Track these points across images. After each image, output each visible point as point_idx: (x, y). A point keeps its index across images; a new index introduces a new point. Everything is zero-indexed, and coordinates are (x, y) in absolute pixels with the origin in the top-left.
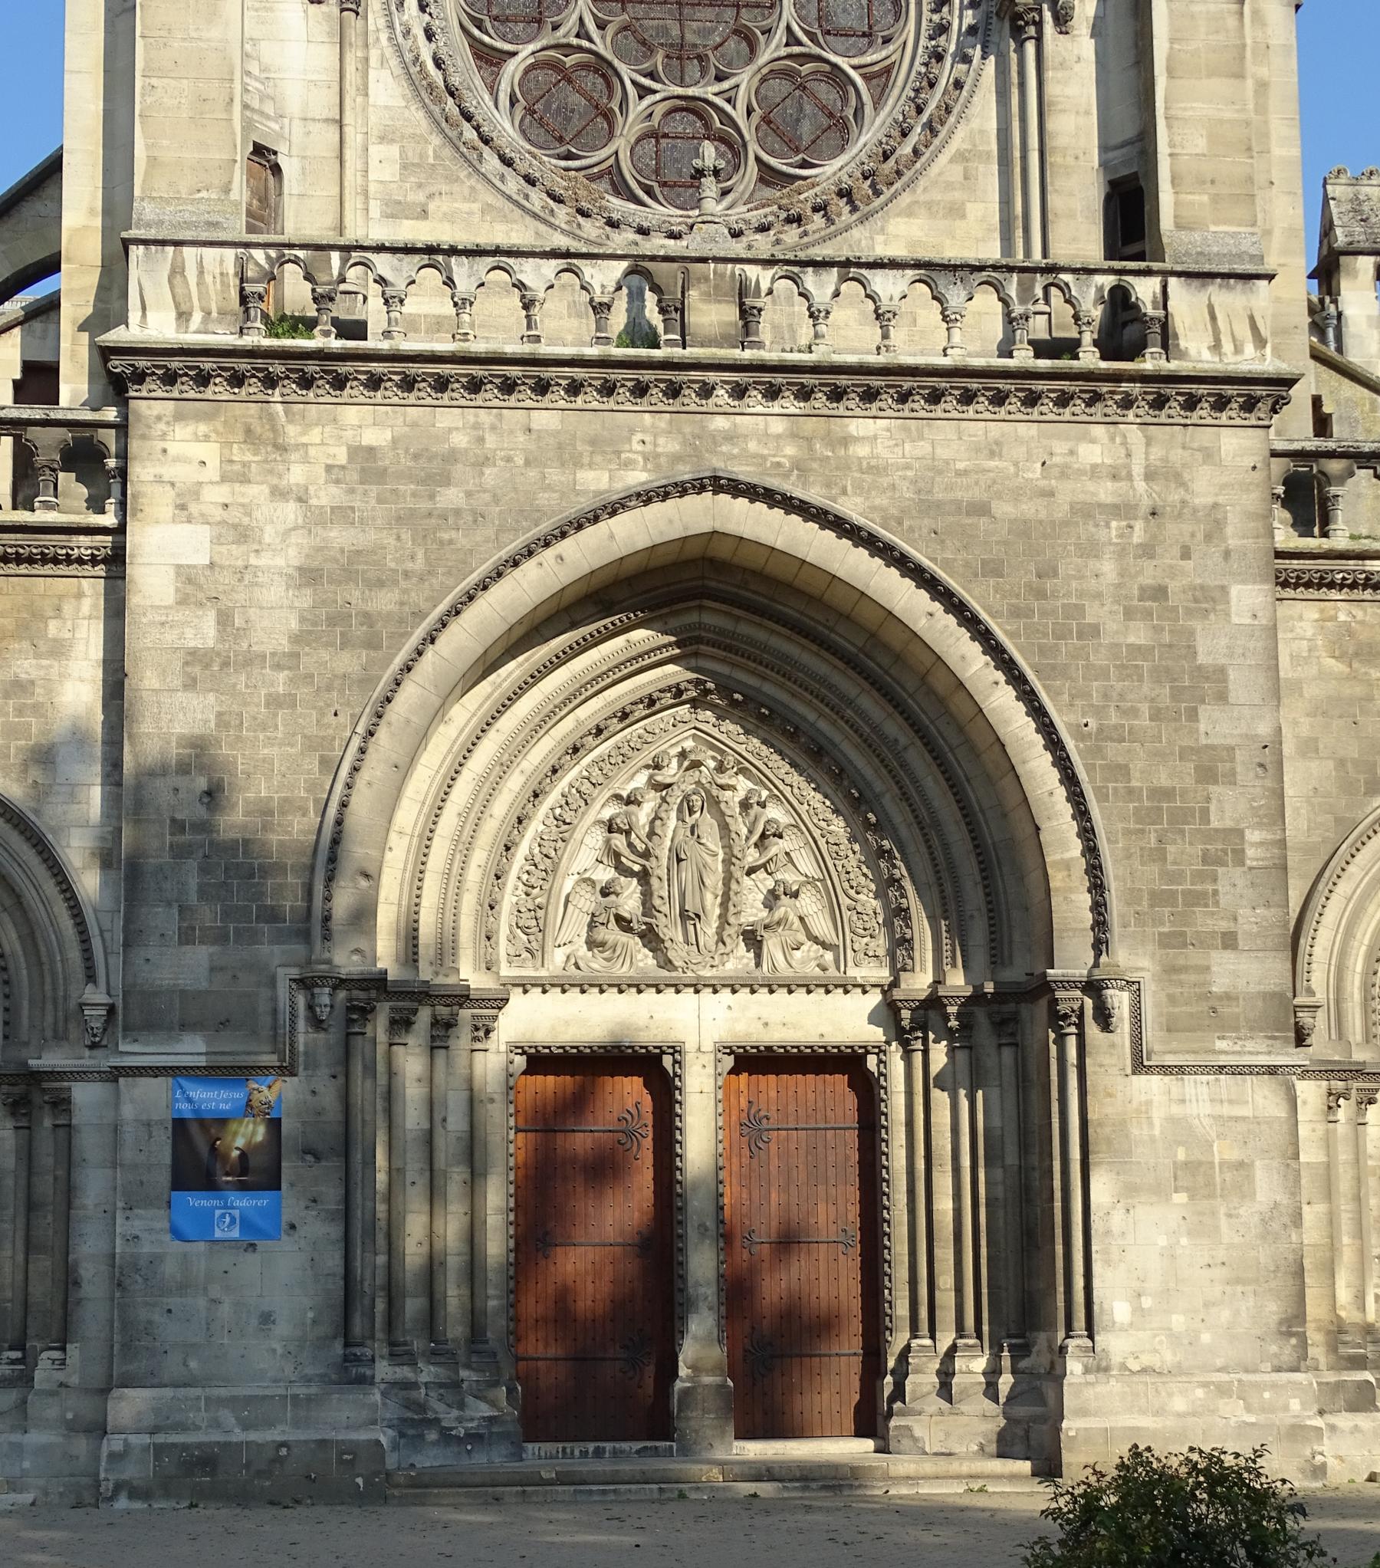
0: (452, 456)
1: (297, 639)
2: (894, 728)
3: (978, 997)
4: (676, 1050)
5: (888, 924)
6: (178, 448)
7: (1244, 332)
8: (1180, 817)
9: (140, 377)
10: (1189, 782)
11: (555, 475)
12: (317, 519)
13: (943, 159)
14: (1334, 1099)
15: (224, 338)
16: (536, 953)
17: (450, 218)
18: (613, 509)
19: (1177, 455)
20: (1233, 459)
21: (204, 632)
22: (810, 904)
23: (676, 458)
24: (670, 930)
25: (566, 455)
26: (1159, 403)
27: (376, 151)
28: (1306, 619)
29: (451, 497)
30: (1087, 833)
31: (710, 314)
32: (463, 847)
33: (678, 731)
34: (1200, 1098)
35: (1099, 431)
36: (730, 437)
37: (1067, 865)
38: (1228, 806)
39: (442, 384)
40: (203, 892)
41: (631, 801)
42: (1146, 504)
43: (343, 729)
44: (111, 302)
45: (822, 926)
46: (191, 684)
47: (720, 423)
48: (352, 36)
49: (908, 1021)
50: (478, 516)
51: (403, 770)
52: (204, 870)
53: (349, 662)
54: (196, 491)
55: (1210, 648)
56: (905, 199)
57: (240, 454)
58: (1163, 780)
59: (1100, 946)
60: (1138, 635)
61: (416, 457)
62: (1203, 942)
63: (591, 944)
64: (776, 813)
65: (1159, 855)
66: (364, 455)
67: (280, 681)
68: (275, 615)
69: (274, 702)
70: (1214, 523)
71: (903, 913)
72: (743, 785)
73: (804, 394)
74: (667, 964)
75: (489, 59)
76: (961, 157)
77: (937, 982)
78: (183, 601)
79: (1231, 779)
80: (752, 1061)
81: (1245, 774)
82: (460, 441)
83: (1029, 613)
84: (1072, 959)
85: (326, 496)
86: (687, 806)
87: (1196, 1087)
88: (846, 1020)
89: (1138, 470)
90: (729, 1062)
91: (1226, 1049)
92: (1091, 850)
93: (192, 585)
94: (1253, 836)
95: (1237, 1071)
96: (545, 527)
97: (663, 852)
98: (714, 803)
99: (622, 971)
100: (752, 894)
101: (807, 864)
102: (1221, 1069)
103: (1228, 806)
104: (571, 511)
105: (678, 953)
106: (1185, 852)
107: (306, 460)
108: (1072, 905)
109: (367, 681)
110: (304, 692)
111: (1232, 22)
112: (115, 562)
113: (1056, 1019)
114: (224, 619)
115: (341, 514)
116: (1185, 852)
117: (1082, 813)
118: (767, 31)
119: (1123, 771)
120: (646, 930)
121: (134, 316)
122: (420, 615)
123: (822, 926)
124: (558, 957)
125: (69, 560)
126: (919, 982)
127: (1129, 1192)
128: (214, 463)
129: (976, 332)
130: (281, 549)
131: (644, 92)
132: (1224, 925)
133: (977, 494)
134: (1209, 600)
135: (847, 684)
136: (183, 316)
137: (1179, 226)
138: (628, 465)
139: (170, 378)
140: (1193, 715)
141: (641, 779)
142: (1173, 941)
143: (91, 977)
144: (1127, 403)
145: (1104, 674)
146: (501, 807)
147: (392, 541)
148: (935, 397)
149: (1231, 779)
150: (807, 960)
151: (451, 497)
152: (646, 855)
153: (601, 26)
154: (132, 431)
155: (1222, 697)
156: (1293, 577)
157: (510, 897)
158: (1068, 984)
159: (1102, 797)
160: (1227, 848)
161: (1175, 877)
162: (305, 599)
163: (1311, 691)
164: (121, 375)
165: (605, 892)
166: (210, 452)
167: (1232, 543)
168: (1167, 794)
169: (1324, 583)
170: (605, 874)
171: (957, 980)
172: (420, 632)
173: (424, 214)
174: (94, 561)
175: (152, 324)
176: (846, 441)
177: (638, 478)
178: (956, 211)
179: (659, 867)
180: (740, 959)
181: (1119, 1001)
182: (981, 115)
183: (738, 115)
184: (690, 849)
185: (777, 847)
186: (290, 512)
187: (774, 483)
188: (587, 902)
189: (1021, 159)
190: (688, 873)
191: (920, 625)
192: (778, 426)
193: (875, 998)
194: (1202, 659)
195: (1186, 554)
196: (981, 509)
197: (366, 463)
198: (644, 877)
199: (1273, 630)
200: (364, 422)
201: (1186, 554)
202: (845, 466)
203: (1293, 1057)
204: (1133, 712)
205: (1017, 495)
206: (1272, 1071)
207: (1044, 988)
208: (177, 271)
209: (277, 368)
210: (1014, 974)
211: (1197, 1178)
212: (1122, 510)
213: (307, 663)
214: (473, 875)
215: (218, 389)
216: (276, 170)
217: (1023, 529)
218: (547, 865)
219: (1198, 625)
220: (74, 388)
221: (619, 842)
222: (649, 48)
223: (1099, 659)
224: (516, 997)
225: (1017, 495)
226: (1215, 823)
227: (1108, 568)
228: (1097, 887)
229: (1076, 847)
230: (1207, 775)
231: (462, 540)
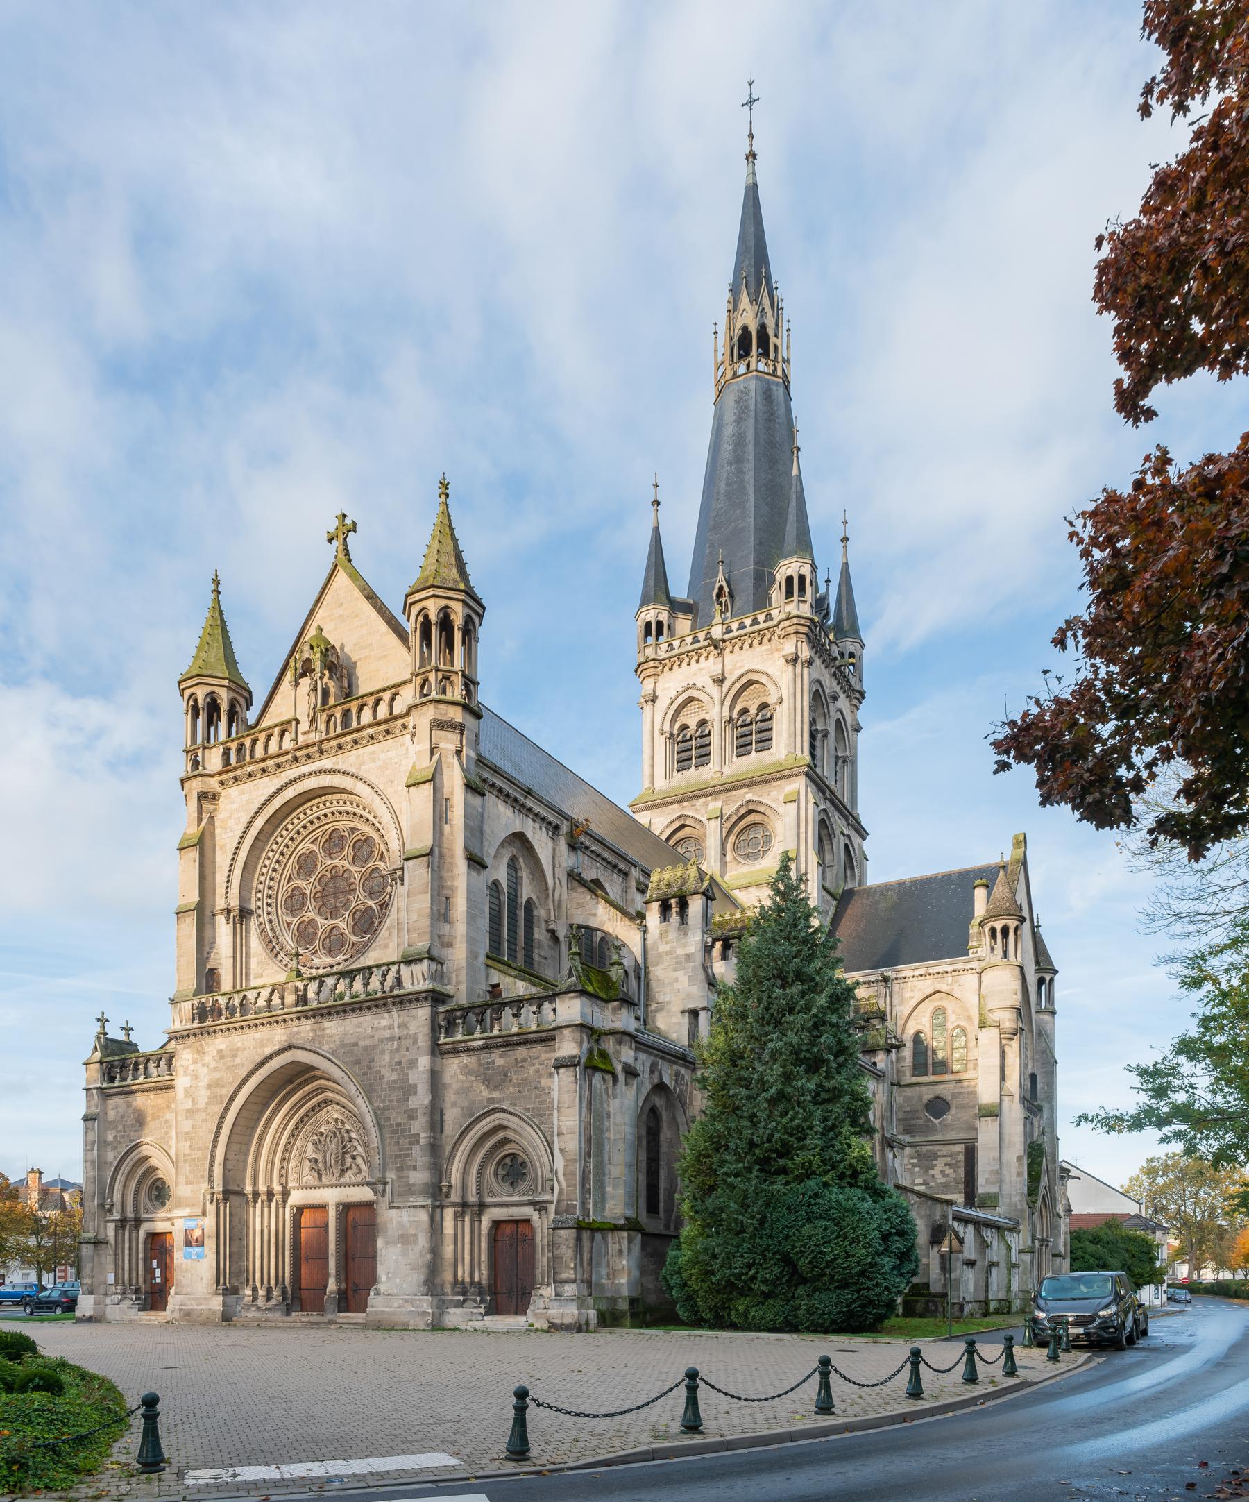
0: (237, 1050)
6: (184, 1056)
7: (420, 977)
8: (403, 1131)
11: (259, 1051)
19: (406, 1019)
21: (189, 1105)
29: (238, 1060)
34: (405, 1215)
35: (386, 1015)
36: (297, 1033)
47: (295, 1029)
54: (187, 1068)
55: (413, 1078)
57: (197, 1056)
58: (399, 1121)
60: (394, 1077)
62: (408, 1169)
65: (397, 1143)
66: (220, 1051)
68: (203, 1096)
69: (203, 1121)
73: (314, 1016)
76: (388, 928)
79: (417, 1118)
81: (420, 1116)
82: (239, 1045)
87: (405, 1212)
91: (413, 1201)
94: (422, 1135)
95: (414, 1207)
106: (404, 1142)
115: (216, 1069)
116: (404, 1142)
119: (389, 1119)
127: (387, 1243)
134: (413, 1063)
142: (400, 1169)
149: (417, 1118)
155: (415, 1093)
161: (401, 1150)
163: (456, 1086)
166: (190, 1056)
168: (399, 1125)
178: (386, 946)
186: (205, 1070)
192: (308, 1028)
196: (356, 1044)
200: (219, 1043)
202: (323, 1036)
204: (391, 1101)
205: (365, 1038)
206: (423, 1207)
211: (404, 1239)
212: (391, 1039)
217: (366, 1048)
225: (365, 1038)
227: (387, 1057)
230: (411, 1118)
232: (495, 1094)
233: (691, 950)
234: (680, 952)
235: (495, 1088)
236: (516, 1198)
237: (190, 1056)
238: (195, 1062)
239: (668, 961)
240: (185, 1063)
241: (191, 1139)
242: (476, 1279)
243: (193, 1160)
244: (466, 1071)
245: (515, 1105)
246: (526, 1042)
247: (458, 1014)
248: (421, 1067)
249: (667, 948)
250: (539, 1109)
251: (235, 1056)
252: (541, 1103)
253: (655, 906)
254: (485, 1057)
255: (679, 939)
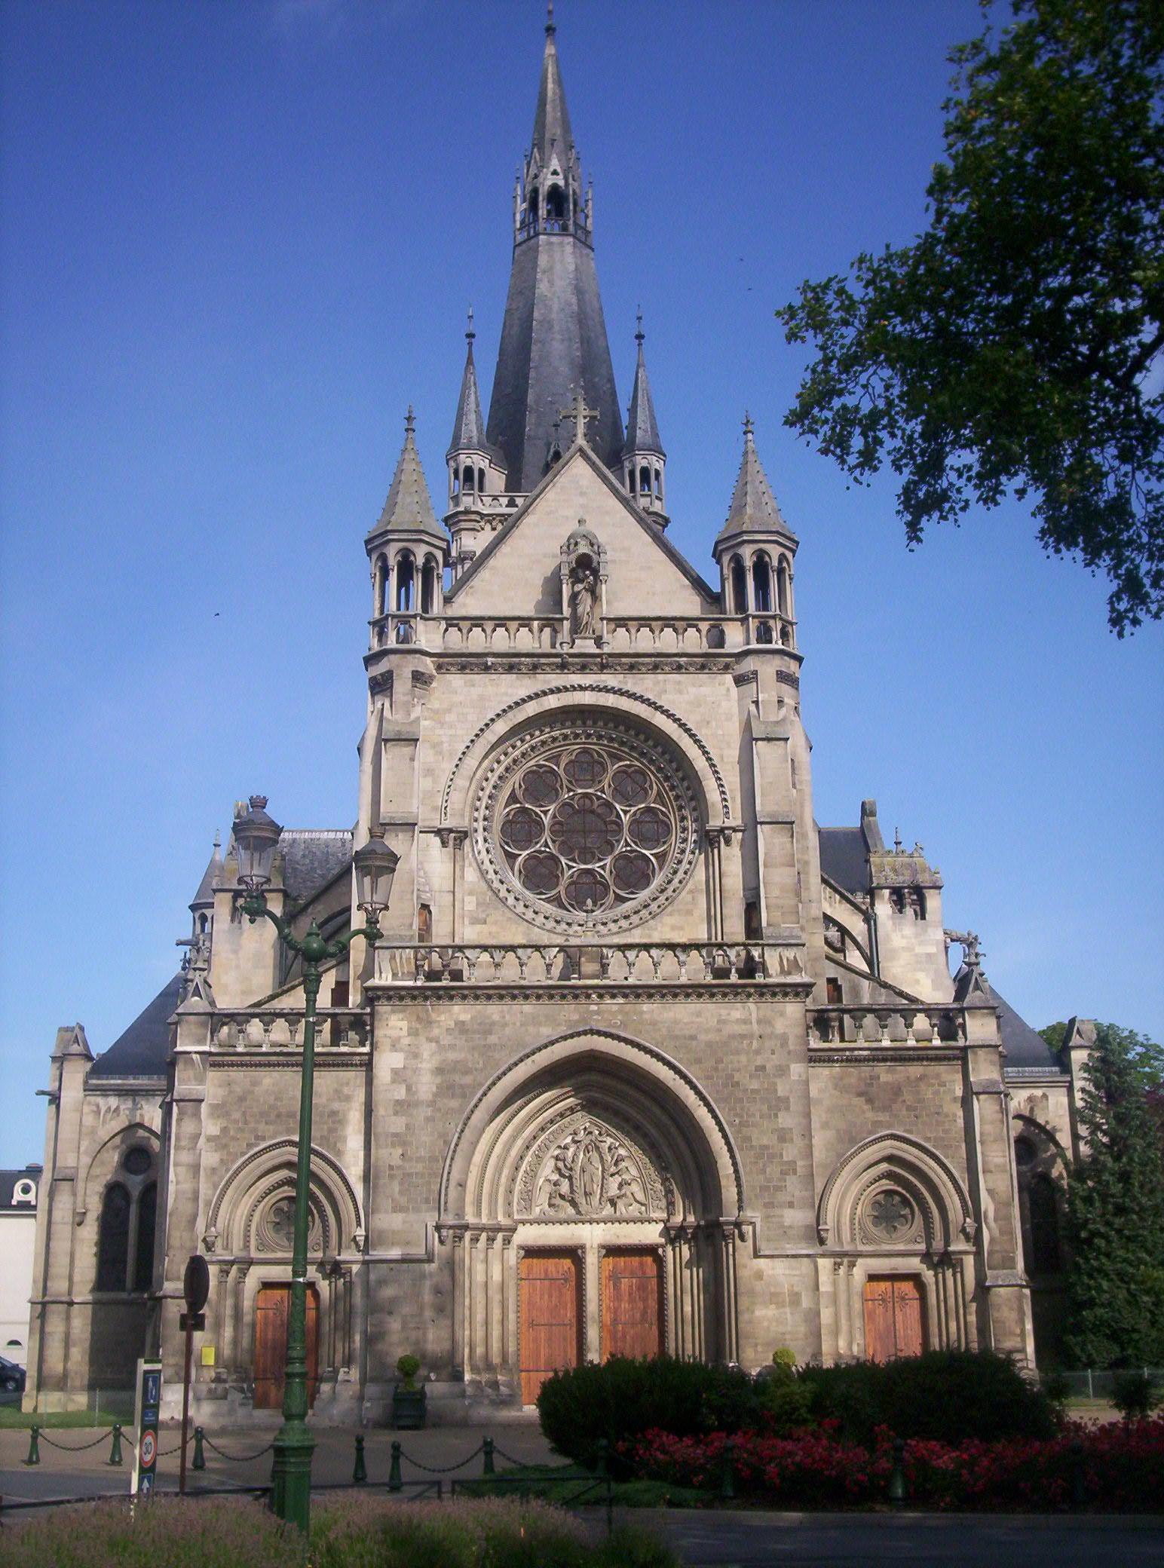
0: (493, 1023)
1: (435, 1095)
2: (665, 1119)
3: (698, 1226)
4: (583, 1247)
5: (666, 1196)
6: (393, 1024)
8: (771, 1157)
9: (379, 998)
10: (775, 1142)
11: (531, 1029)
12: (442, 1048)
13: (684, 893)
14: (837, 1266)
15: (410, 983)
16: (528, 1208)
17: (495, 923)
18: (552, 1043)
20: (791, 1013)
21: (401, 1093)
22: (635, 1188)
23: (577, 1021)
24: (581, 1200)
25: (535, 1021)
26: (762, 995)
27: (467, 899)
28: (823, 1075)
29: (493, 1039)
30: (735, 1164)
31: (589, 967)
32: (499, 1170)
33: (582, 1121)
36: (597, 1013)
37: (728, 1176)
38: (791, 1152)
39: (489, 997)
40: (401, 1192)
41: (566, 1148)
42: (757, 1033)
43: (454, 1128)
44: (368, 972)
45: (640, 1196)
46: (396, 1113)
47: (594, 1008)
48: (458, 858)
49: (674, 1235)
50: (503, 1046)
51: (474, 1145)
52: (401, 1184)
53: (454, 1103)
56: (670, 908)
58: (765, 1142)
59: (740, 1208)
60: (755, 1085)
61: (480, 1024)
62: (781, 1206)
63: (550, 1205)
64: (622, 1152)
67: (429, 1112)
68: (426, 1086)
70: (784, 1039)
71: (671, 1192)
72: (609, 1140)
73: (625, 996)
74: (579, 1213)
75: (511, 858)
76: (691, 892)
77: (684, 1219)
78: (393, 1081)
80: (613, 1251)
82: (496, 1017)
83: (712, 1078)
84: (730, 1214)
85: (446, 1040)
86: (587, 1150)
88: (651, 1234)
89: (754, 1021)
90: (604, 1252)
92: (736, 1171)
93: (397, 1075)
94: (800, 1163)
96: (528, 1050)
97: (578, 1169)
98: (597, 1148)
99: (562, 1215)
100: (613, 1184)
101: (634, 1171)
102: (787, 1256)
103: (791, 1152)
104: (535, 1046)
105: (583, 1208)
107: (439, 1027)
108: (729, 1193)
109: (461, 1110)
110: (438, 1115)
111: (789, 845)
112: (368, 1065)
113: (725, 1237)
114: (409, 1089)
115: (452, 1047)
117: (733, 1157)
118: (618, 841)
119: (749, 1139)
120: (571, 1201)
121: (377, 975)
122: (481, 1085)
123: (640, 1196)
124: (538, 1210)
125: (352, 1065)
126: (678, 1219)
128: (405, 1029)
129: (694, 969)
130: (429, 1059)
131: (570, 867)
132: (789, 1199)
133: (693, 1032)
134: (783, 1071)
135: (648, 1103)
136: (395, 975)
137: (769, 925)
138: (559, 1025)
139: (389, 998)
140: (776, 1116)
141: (569, 1140)
142: (769, 1205)
143: (359, 1224)
144: (749, 995)
145: (741, 1100)
146: (514, 1152)
147: (470, 1057)
148: (675, 996)
150: (634, 1210)
151: (493, 1039)
152: (571, 1169)
153: (554, 842)
154: (377, 1017)
155: (787, 1109)
156: (815, 1058)
157: (518, 1187)
158: (728, 1223)
159: (741, 1149)
160: (790, 1168)
161: (769, 1180)
162: (438, 1080)
164: (372, 996)
165: (555, 1184)
166: (404, 1024)
167: (791, 1048)
168: (766, 1147)
169: (830, 1060)
170: (555, 1177)
171: (691, 1219)
172: (481, 1092)
173: (485, 922)
174: (361, 1065)
175: (383, 979)
176: (642, 1012)
177: (563, 1030)
178: (689, 913)
179: (577, 1174)
180: (608, 1210)
181: (747, 1229)
182: (700, 874)
183: (606, 875)
184: (589, 1168)
185: (623, 1164)
187: (613, 1031)
188: (548, 1188)
189: (714, 891)
190: (587, 1177)
191: (670, 1084)
192: (615, 1008)
193: (661, 1226)
194: (780, 1094)
195: (773, 1053)
196: (693, 1038)
197: (461, 1027)
198: (570, 1178)
199: (807, 1083)
200: (460, 1012)
201: (773, 1053)
203: (819, 1250)
204: (753, 1115)
205: (707, 1031)
206: (808, 1256)
207: (719, 1225)
208: (393, 958)
209: (429, 993)
210: (711, 1217)
212: (749, 1036)
213: (439, 1104)
214: (503, 1180)
215: (408, 1001)
216: (430, 912)
218: (532, 1174)
219: (778, 1081)
220: (354, 998)
221: (560, 1164)
222: (571, 850)
223: (740, 1095)
224: (520, 1227)
226: (785, 1159)
228: (739, 1186)
229: (731, 1170)
231: (497, 1056)
232: (883, 1117)
233: (933, 950)
234: (919, 950)
235: (885, 1108)
236: (901, 1247)
237: (404, 1024)
238: (413, 1033)
239: (904, 958)
240: (394, 1033)
241: (404, 1144)
242: (855, 1349)
243: (410, 1175)
244: (839, 1085)
245: (910, 1132)
246: (920, 1059)
247: (833, 1015)
248: (795, 1077)
249: (903, 943)
250: (942, 1139)
251: (489, 1032)
252: (945, 1131)
253: (887, 892)
254: (865, 1070)
255: (917, 936)
